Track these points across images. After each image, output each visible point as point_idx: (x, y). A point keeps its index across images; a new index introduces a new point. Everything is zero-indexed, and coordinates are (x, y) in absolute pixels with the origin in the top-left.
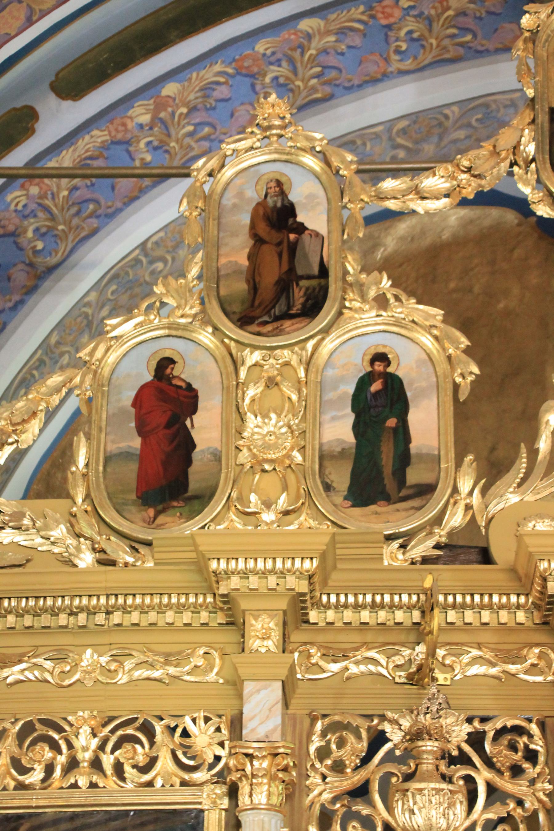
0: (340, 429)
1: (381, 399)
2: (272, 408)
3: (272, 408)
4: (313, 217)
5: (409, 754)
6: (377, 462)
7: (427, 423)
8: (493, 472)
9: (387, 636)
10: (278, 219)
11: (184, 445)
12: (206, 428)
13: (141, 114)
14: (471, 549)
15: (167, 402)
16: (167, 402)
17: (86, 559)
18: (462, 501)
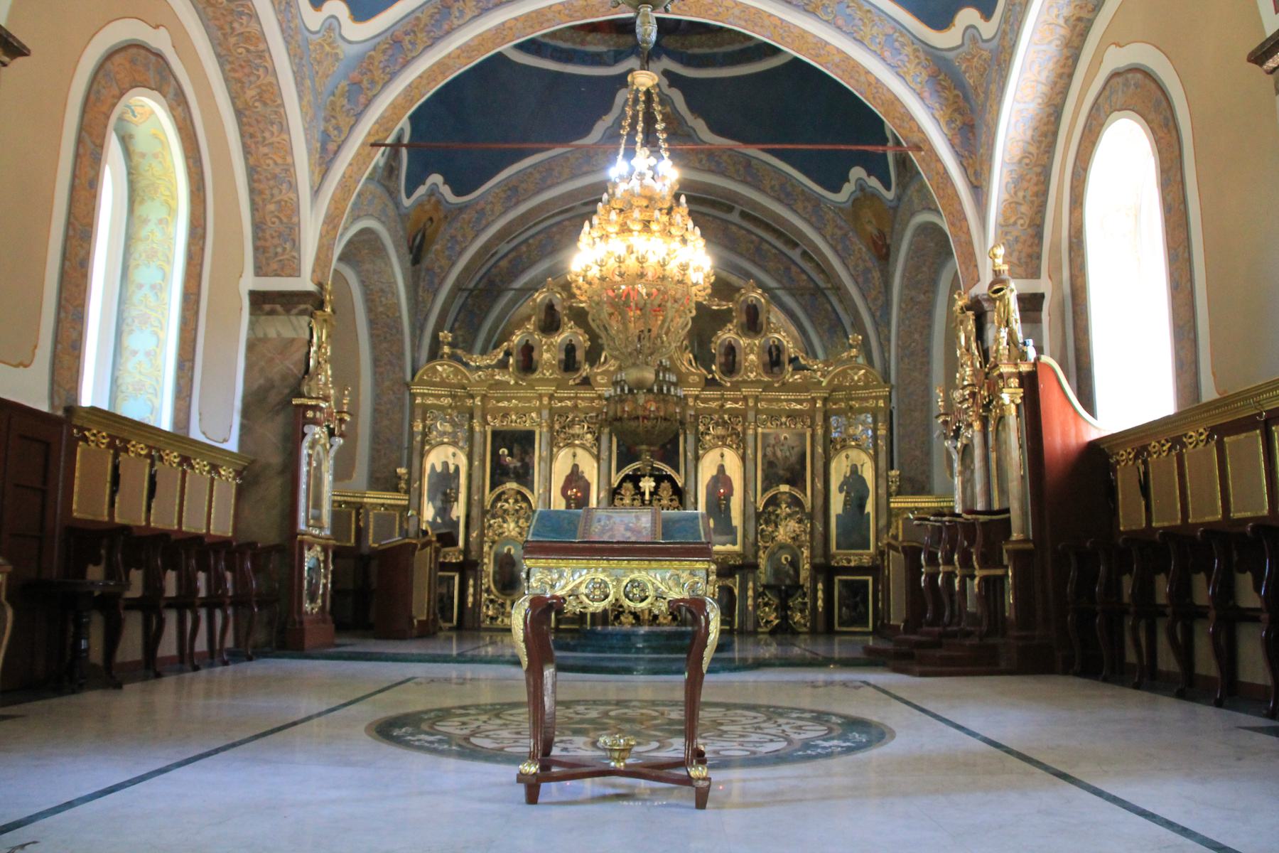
0: (563, 356)
1: (570, 349)
2: (549, 352)
3: (549, 352)
4: (558, 308)
5: (573, 420)
6: (569, 364)
7: (580, 355)
8: (592, 365)
9: (569, 398)
10: (550, 308)
11: (531, 359)
12: (535, 355)
13: (524, 248)
14: (586, 382)
15: (528, 350)
16: (528, 350)
17: (512, 382)
18: (586, 370)
